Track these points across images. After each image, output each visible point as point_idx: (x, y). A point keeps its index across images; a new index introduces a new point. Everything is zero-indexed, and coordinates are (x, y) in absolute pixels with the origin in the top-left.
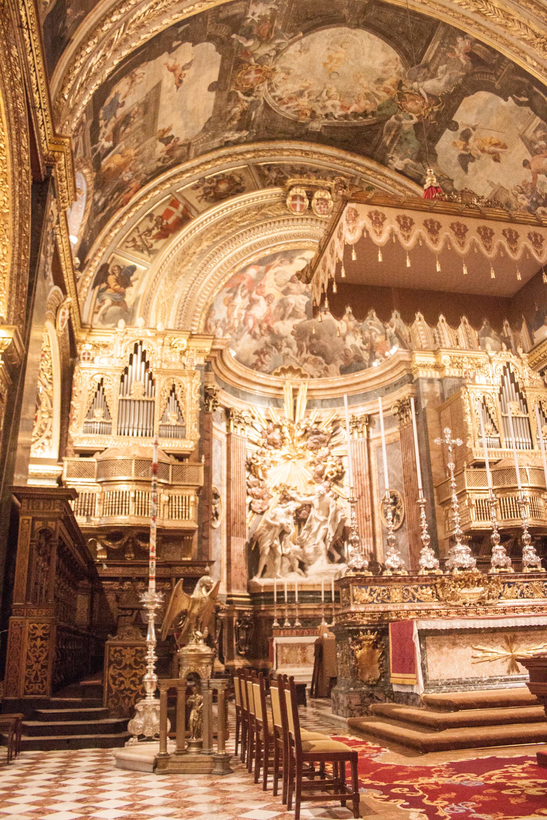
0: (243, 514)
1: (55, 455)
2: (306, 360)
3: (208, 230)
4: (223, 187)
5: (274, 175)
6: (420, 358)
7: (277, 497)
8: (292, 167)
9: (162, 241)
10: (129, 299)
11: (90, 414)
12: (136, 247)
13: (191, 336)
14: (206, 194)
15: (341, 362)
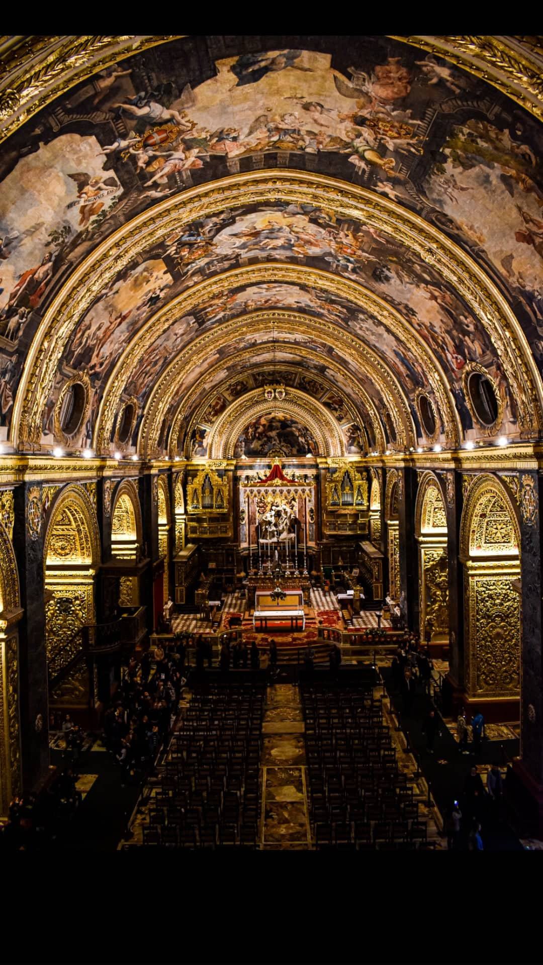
0: (255, 515)
1: (183, 512)
2: (283, 446)
3: (233, 411)
4: (239, 388)
5: (261, 378)
6: (319, 460)
7: (269, 506)
8: (269, 372)
9: (215, 417)
10: (205, 444)
11: (193, 502)
12: (206, 421)
13: (228, 459)
14: (232, 392)
15: (297, 447)
